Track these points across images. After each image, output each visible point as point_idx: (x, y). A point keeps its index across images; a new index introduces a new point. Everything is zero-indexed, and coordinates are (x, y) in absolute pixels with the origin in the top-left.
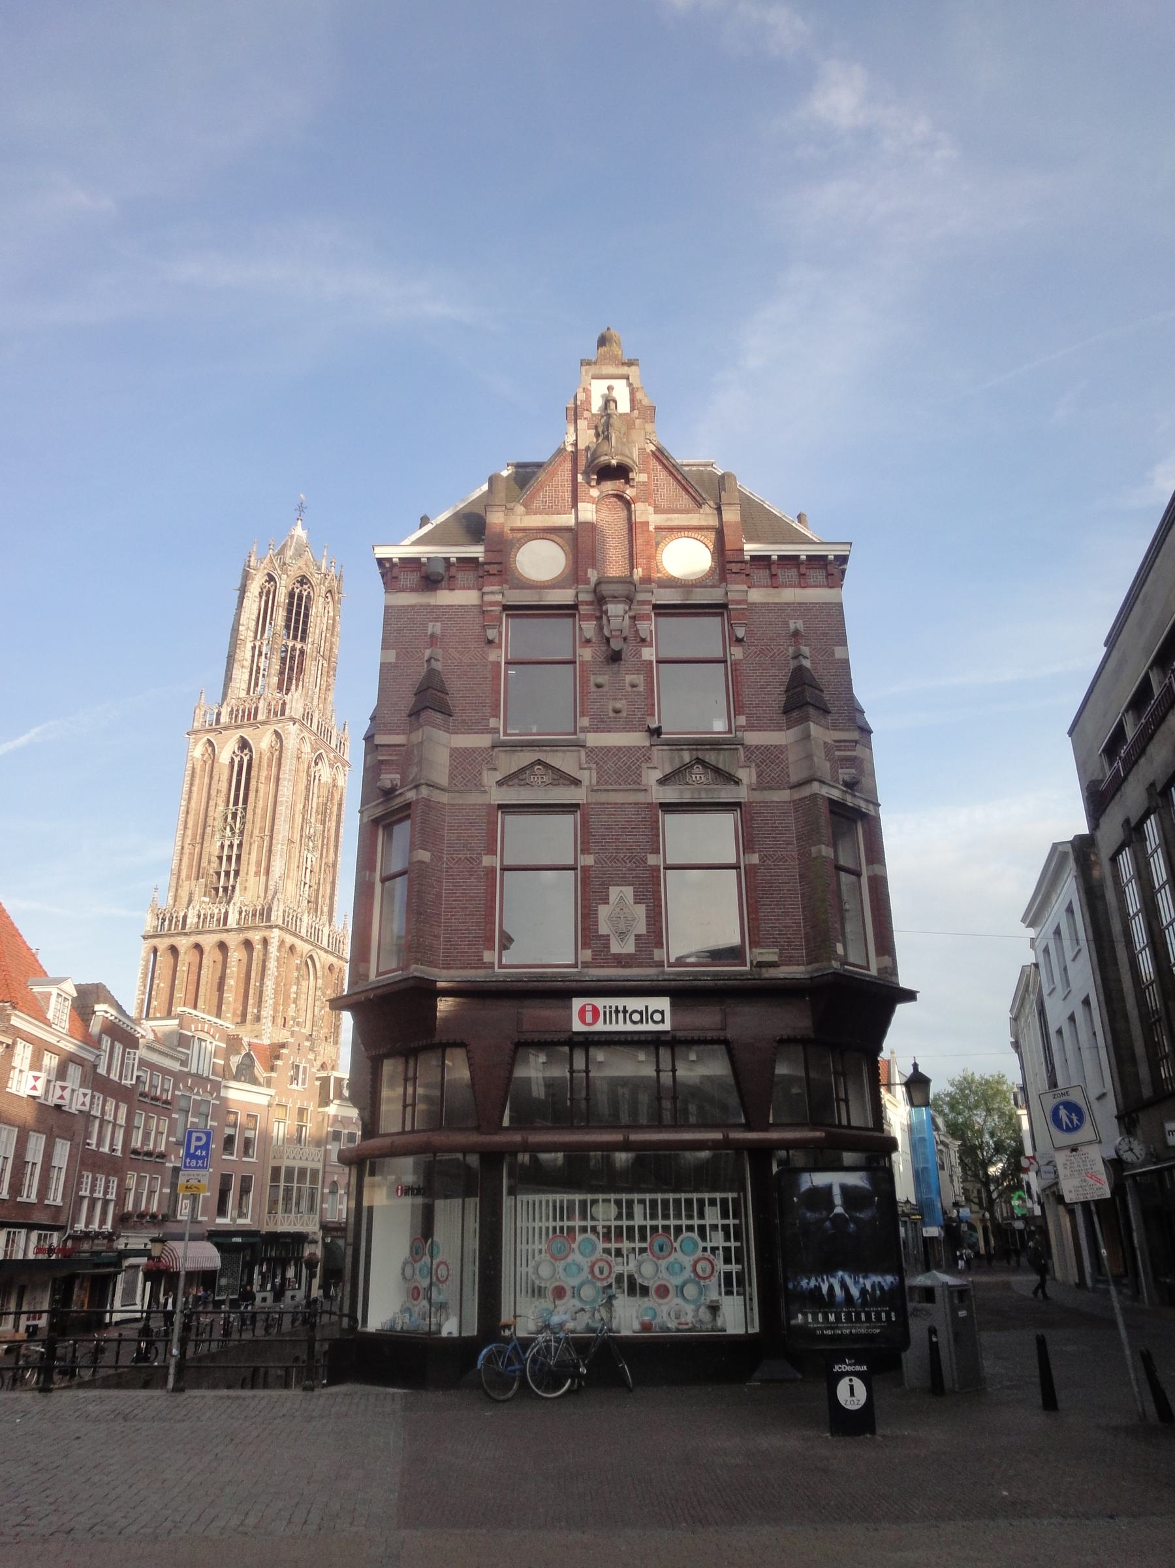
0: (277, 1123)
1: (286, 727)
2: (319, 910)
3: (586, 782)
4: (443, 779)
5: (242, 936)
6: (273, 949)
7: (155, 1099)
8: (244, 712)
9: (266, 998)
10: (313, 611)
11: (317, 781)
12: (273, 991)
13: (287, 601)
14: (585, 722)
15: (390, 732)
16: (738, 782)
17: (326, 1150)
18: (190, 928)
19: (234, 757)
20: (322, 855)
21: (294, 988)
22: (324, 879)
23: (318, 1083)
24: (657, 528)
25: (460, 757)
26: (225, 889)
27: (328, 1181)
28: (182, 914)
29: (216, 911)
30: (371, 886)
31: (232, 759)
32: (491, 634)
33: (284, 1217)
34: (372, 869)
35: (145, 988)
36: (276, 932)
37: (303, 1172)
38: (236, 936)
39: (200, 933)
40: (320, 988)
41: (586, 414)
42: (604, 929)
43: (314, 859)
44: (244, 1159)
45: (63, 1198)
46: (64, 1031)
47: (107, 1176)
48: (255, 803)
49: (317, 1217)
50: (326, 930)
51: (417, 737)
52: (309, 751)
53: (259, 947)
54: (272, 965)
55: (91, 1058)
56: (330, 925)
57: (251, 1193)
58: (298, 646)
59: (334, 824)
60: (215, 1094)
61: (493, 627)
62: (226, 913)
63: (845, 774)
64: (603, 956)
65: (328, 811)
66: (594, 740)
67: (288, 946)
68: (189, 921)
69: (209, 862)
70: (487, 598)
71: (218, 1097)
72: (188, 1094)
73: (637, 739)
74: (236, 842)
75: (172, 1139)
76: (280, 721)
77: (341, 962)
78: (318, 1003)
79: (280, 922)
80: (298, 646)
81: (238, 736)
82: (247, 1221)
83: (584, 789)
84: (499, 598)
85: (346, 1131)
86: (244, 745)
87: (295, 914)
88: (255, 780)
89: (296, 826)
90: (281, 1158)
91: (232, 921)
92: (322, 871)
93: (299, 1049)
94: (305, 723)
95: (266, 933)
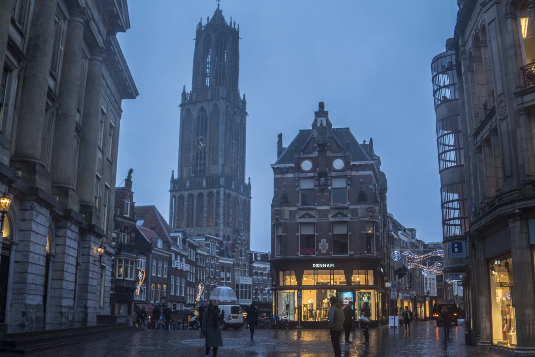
1: (221, 101)
3: (317, 217)
4: (288, 218)
5: (209, 190)
6: (222, 196)
11: (234, 123)
14: (316, 204)
15: (277, 207)
16: (348, 217)
17: (253, 278)
21: (231, 211)
22: (240, 164)
23: (249, 256)
24: (332, 157)
26: (200, 171)
29: (197, 180)
30: (274, 238)
32: (296, 184)
34: (274, 234)
36: (222, 189)
37: (246, 285)
41: (316, 127)
42: (320, 248)
43: (235, 156)
45: (184, 295)
46: (181, 248)
47: (192, 288)
49: (252, 300)
51: (282, 208)
52: (230, 110)
53: (215, 195)
54: (222, 202)
55: (187, 255)
60: (217, 262)
61: (297, 183)
63: (370, 214)
64: (320, 253)
65: (240, 135)
66: (318, 208)
69: (193, 160)
70: (295, 176)
71: (218, 262)
72: (210, 262)
73: (327, 208)
74: (203, 151)
75: (207, 276)
77: (248, 199)
78: (240, 216)
79: (224, 184)
81: (200, 105)
83: (316, 219)
84: (298, 176)
85: (259, 272)
86: (202, 109)
90: (239, 281)
91: (204, 183)
92: (239, 161)
93: (242, 245)
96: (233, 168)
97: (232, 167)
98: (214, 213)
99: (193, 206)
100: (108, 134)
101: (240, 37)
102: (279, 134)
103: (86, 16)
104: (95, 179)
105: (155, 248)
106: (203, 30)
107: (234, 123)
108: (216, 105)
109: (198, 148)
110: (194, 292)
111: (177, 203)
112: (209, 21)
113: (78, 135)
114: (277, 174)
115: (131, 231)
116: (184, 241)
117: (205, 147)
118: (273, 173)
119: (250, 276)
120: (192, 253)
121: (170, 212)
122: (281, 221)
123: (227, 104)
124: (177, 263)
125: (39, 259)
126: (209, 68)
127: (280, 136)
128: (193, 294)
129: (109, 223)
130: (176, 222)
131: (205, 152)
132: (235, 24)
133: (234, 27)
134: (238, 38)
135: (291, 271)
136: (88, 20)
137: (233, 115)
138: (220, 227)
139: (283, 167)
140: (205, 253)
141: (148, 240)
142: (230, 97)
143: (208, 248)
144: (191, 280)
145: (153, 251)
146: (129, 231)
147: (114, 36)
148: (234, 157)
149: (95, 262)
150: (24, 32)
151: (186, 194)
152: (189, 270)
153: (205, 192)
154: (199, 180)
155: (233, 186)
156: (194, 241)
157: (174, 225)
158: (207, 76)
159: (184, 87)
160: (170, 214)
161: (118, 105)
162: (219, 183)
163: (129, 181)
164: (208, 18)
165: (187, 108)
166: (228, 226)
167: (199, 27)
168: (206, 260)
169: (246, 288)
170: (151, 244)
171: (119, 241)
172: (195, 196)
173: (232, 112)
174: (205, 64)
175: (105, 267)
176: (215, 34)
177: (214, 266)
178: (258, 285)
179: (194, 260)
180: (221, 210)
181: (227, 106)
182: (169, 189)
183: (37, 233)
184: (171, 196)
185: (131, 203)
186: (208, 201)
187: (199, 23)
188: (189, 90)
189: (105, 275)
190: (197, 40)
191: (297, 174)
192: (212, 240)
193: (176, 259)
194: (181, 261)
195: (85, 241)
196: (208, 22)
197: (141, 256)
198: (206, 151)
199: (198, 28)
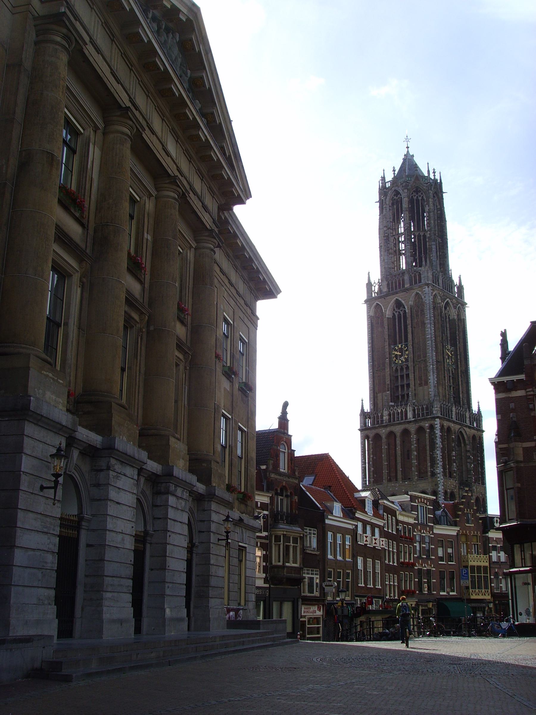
0: (462, 545)
1: (424, 290)
2: (461, 402)
5: (417, 425)
6: (438, 432)
7: (406, 538)
8: (396, 283)
9: (438, 462)
10: (427, 209)
11: (447, 320)
12: (441, 457)
13: (410, 206)
17: (489, 556)
18: (386, 422)
19: (395, 313)
20: (457, 366)
25: (525, 449)
26: (403, 396)
27: (493, 572)
28: (380, 415)
29: (399, 411)
30: (504, 491)
31: (393, 313)
32: (531, 406)
33: (473, 591)
35: (365, 460)
37: (479, 567)
38: (414, 425)
39: (393, 425)
40: (469, 451)
44: (449, 563)
45: (381, 586)
48: (413, 340)
49: (489, 591)
50: (467, 415)
51: (511, 445)
52: (440, 301)
53: (428, 430)
54: (438, 441)
55: (382, 524)
56: (469, 411)
57: (455, 580)
58: (422, 234)
59: (462, 344)
61: (532, 404)
62: (406, 411)
65: (457, 337)
67: (446, 428)
68: (384, 418)
71: (433, 534)
72: (419, 533)
74: (404, 367)
76: (420, 287)
80: (422, 234)
81: (395, 299)
82: (454, 593)
84: (532, 393)
85: (499, 546)
86: (398, 304)
87: (447, 407)
88: (410, 326)
89: (439, 351)
90: (468, 561)
91: (410, 415)
92: (460, 377)
94: (434, 285)
95: (432, 422)
96: (452, 388)
97: (450, 386)
98: (428, 458)
99: (395, 450)
100: (238, 352)
101: (444, 191)
102: (502, 332)
103: (180, 188)
104: (223, 420)
105: (329, 517)
106: (389, 187)
107: (447, 320)
108: (417, 294)
109: (396, 362)
110: (396, 581)
111: (371, 446)
112: (396, 172)
113: (185, 358)
114: (500, 392)
115: (291, 493)
116: (376, 504)
117: (407, 360)
118: (493, 391)
119: (485, 554)
120: (390, 521)
121: (362, 462)
122: (512, 465)
123: (434, 294)
124: (366, 537)
125: (123, 539)
126: (403, 242)
127: (504, 335)
128: (396, 584)
129: (249, 483)
130: (372, 476)
131: (407, 368)
132: (434, 172)
133: (435, 178)
134: (442, 192)
135: (533, 543)
136: (184, 194)
137: (445, 308)
138: (438, 479)
139: (507, 381)
140: (412, 521)
141: (319, 506)
142: (438, 281)
143: (417, 513)
144: (391, 563)
145: (327, 521)
146: (289, 494)
147: (230, 211)
148: (452, 371)
149: (220, 541)
150: (85, 221)
151: (383, 432)
152: (387, 548)
153: (412, 428)
154: (402, 410)
155: (454, 416)
156: (393, 503)
157: (369, 481)
158: (400, 254)
159: (369, 274)
160: (362, 465)
161: (252, 310)
162: (432, 413)
163: (283, 420)
164: (394, 168)
165: (375, 304)
166: (450, 476)
167: (382, 183)
168: (414, 531)
169: (479, 571)
170: (324, 511)
171: (274, 509)
172: (398, 435)
173: (443, 304)
174: (396, 238)
175: (245, 548)
176: (406, 191)
177: (427, 540)
178: (498, 566)
179: (394, 533)
180: (438, 453)
181: (435, 296)
182: (359, 427)
183: (118, 503)
184: (361, 437)
185: (290, 451)
186: (418, 440)
187: (382, 177)
188: (376, 276)
189: (246, 560)
190: (382, 203)
191: (531, 389)
192: (421, 500)
193: (365, 531)
194: (373, 534)
195: (204, 510)
196: (394, 174)
197: (310, 530)
198: (409, 365)
199: (381, 185)
